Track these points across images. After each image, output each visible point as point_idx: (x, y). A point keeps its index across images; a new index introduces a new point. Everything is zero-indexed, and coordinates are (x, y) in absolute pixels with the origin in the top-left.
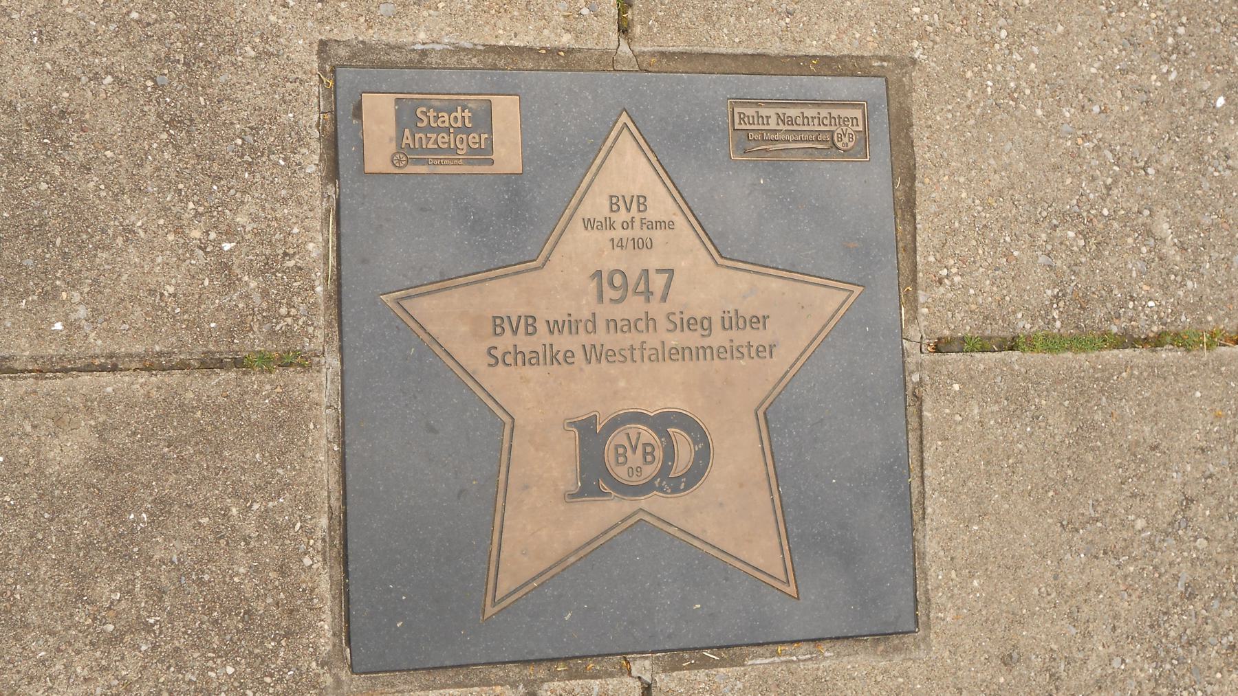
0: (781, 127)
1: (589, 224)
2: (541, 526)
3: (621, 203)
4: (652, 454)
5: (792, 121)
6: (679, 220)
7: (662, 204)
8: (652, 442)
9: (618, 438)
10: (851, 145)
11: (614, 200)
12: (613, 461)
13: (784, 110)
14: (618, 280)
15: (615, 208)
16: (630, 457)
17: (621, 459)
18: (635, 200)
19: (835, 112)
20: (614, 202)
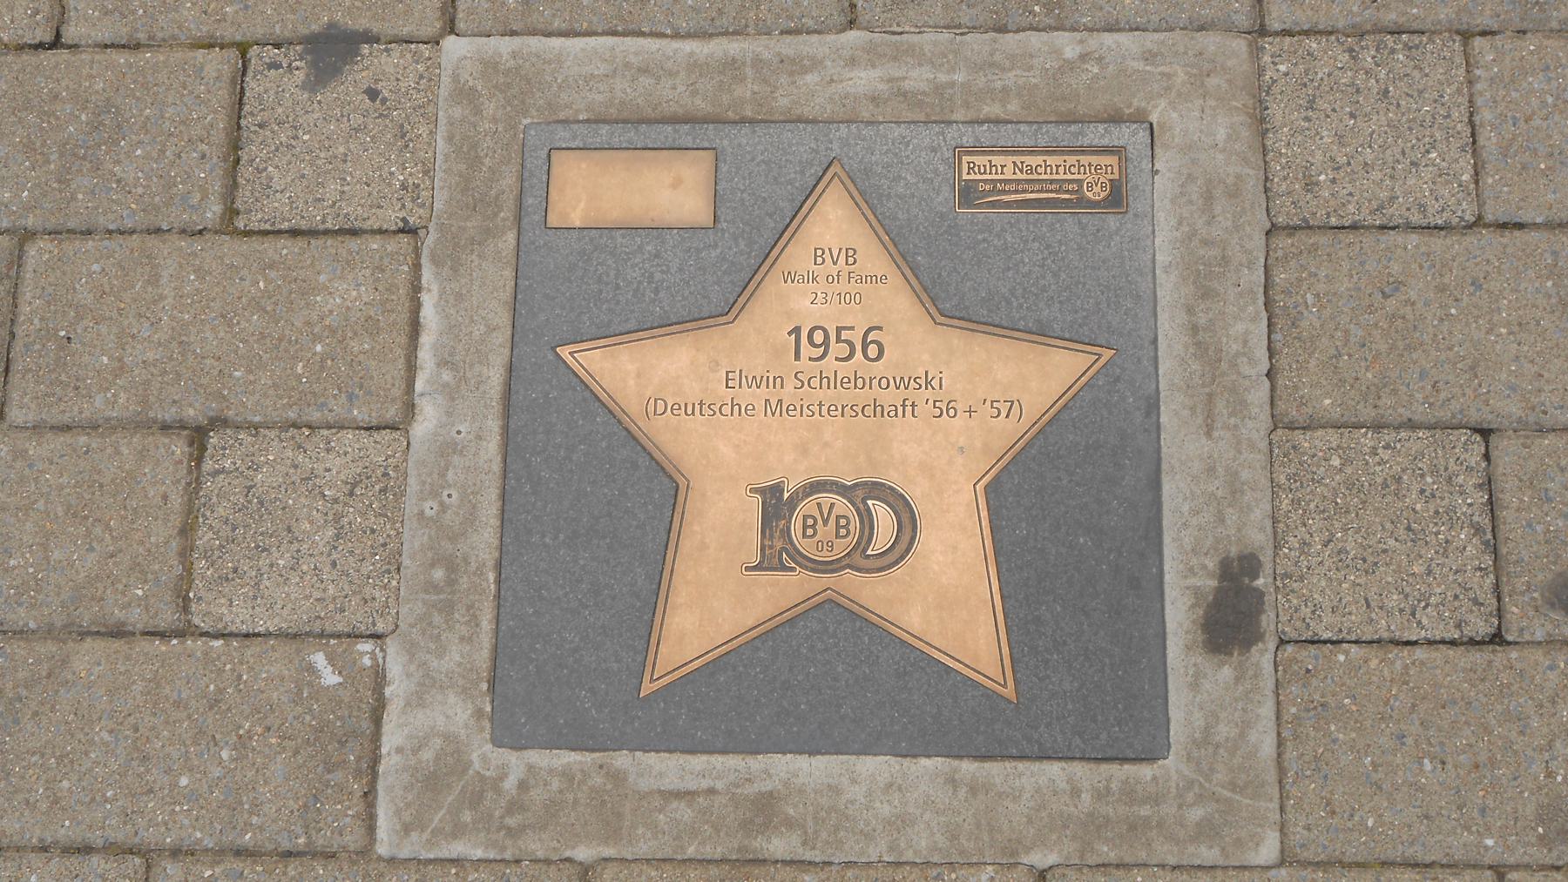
0: (1019, 176)
1: (789, 277)
2: (713, 602)
4: (846, 527)
5: (1031, 170)
7: (873, 259)
9: (807, 506)
10: (1103, 195)
11: (819, 252)
13: (1023, 158)
14: (819, 337)
15: (819, 260)
17: (810, 532)
19: (1085, 159)
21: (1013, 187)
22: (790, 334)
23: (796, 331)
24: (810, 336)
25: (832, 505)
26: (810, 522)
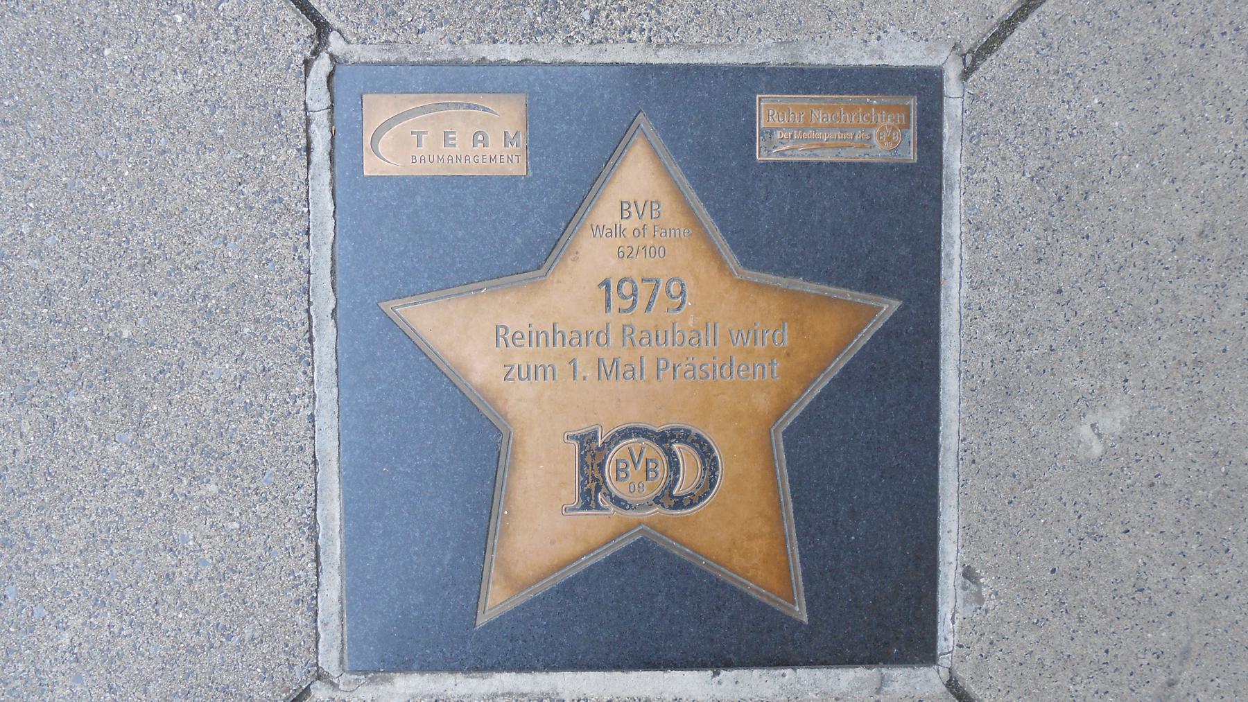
1: (597, 231)
3: (633, 209)
12: (614, 477)
15: (626, 214)
17: (623, 475)
18: (649, 204)
20: (624, 208)
22: (600, 285)
23: (606, 283)
24: (619, 288)
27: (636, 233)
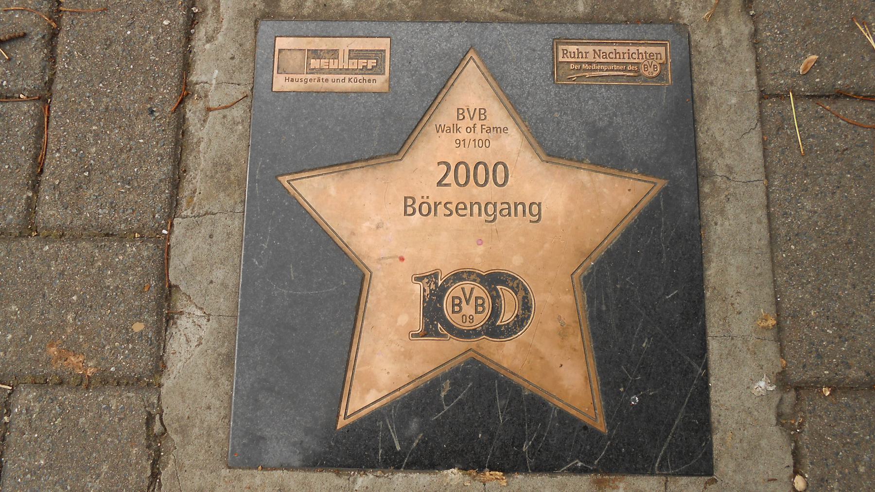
3: (466, 114)
4: (482, 305)
6: (510, 124)
7: (498, 115)
8: (484, 296)
9: (455, 290)
11: (461, 111)
12: (450, 311)
15: (461, 117)
16: (467, 308)
18: (477, 111)
19: (642, 49)
20: (460, 113)
21: (594, 66)
25: (472, 289)
26: (457, 301)
27: (469, 130)
